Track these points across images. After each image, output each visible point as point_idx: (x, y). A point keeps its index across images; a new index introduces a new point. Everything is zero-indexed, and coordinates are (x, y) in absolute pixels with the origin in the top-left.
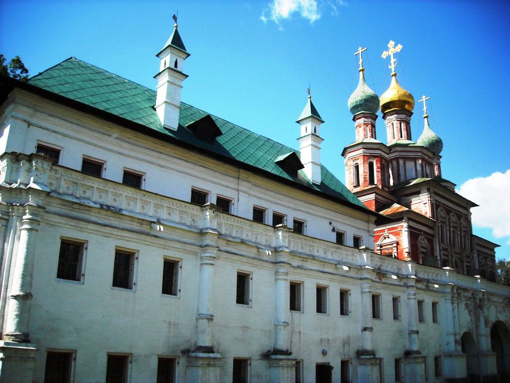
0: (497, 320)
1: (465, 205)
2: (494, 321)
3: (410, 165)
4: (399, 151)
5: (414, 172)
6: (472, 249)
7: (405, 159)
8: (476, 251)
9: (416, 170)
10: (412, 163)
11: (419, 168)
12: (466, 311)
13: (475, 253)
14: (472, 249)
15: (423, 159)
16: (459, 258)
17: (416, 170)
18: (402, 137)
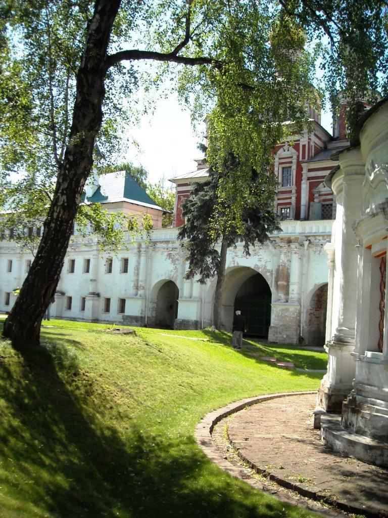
12: (170, 261)
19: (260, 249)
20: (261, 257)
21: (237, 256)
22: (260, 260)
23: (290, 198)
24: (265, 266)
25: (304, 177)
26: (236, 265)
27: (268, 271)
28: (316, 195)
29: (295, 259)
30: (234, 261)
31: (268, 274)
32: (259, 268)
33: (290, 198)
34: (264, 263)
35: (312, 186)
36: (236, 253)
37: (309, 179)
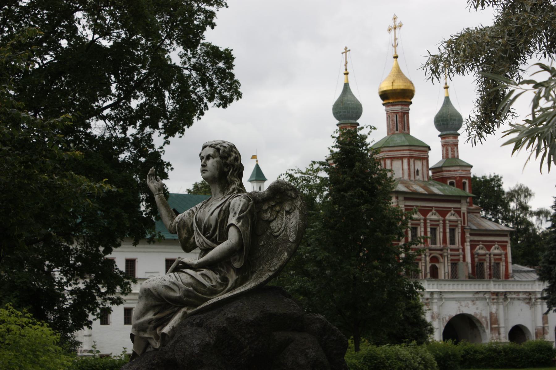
0: (458, 313)
1: (459, 199)
2: (454, 315)
3: (397, 165)
4: (386, 152)
5: (401, 171)
6: (463, 241)
7: (392, 159)
8: (468, 244)
9: (403, 169)
10: (400, 162)
11: (406, 167)
13: (467, 245)
14: (463, 241)
15: (409, 158)
16: (441, 255)
17: (403, 169)
18: (397, 130)
19: (477, 300)
20: (477, 306)
21: (461, 305)
22: (477, 309)
23: (459, 255)
24: (481, 314)
25: (468, 240)
26: (461, 312)
27: (483, 317)
28: (476, 256)
29: (501, 307)
30: (460, 310)
31: (483, 319)
32: (477, 315)
33: (459, 255)
34: (480, 312)
35: (473, 247)
36: (460, 303)
37: (471, 241)
